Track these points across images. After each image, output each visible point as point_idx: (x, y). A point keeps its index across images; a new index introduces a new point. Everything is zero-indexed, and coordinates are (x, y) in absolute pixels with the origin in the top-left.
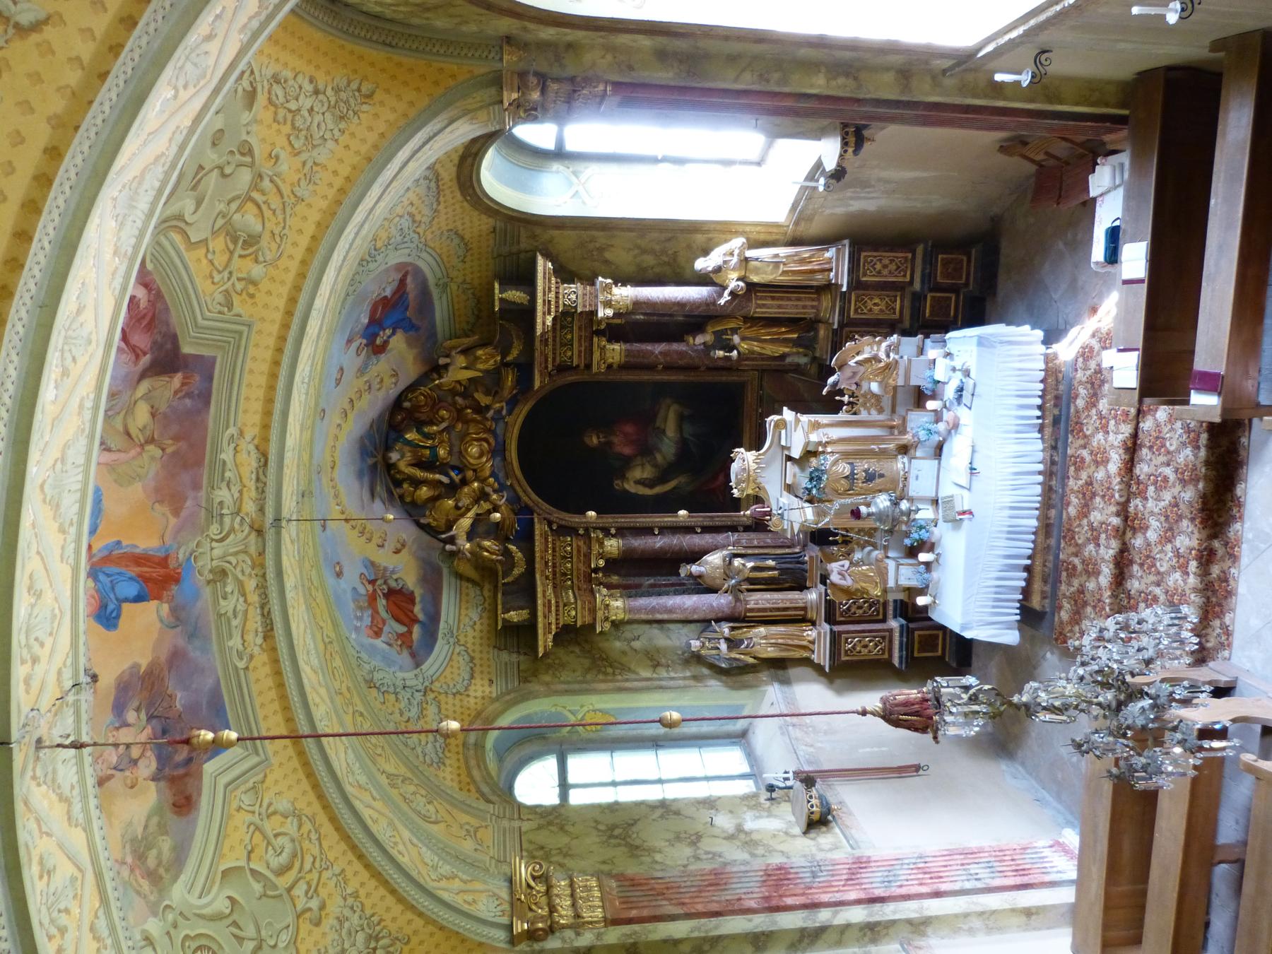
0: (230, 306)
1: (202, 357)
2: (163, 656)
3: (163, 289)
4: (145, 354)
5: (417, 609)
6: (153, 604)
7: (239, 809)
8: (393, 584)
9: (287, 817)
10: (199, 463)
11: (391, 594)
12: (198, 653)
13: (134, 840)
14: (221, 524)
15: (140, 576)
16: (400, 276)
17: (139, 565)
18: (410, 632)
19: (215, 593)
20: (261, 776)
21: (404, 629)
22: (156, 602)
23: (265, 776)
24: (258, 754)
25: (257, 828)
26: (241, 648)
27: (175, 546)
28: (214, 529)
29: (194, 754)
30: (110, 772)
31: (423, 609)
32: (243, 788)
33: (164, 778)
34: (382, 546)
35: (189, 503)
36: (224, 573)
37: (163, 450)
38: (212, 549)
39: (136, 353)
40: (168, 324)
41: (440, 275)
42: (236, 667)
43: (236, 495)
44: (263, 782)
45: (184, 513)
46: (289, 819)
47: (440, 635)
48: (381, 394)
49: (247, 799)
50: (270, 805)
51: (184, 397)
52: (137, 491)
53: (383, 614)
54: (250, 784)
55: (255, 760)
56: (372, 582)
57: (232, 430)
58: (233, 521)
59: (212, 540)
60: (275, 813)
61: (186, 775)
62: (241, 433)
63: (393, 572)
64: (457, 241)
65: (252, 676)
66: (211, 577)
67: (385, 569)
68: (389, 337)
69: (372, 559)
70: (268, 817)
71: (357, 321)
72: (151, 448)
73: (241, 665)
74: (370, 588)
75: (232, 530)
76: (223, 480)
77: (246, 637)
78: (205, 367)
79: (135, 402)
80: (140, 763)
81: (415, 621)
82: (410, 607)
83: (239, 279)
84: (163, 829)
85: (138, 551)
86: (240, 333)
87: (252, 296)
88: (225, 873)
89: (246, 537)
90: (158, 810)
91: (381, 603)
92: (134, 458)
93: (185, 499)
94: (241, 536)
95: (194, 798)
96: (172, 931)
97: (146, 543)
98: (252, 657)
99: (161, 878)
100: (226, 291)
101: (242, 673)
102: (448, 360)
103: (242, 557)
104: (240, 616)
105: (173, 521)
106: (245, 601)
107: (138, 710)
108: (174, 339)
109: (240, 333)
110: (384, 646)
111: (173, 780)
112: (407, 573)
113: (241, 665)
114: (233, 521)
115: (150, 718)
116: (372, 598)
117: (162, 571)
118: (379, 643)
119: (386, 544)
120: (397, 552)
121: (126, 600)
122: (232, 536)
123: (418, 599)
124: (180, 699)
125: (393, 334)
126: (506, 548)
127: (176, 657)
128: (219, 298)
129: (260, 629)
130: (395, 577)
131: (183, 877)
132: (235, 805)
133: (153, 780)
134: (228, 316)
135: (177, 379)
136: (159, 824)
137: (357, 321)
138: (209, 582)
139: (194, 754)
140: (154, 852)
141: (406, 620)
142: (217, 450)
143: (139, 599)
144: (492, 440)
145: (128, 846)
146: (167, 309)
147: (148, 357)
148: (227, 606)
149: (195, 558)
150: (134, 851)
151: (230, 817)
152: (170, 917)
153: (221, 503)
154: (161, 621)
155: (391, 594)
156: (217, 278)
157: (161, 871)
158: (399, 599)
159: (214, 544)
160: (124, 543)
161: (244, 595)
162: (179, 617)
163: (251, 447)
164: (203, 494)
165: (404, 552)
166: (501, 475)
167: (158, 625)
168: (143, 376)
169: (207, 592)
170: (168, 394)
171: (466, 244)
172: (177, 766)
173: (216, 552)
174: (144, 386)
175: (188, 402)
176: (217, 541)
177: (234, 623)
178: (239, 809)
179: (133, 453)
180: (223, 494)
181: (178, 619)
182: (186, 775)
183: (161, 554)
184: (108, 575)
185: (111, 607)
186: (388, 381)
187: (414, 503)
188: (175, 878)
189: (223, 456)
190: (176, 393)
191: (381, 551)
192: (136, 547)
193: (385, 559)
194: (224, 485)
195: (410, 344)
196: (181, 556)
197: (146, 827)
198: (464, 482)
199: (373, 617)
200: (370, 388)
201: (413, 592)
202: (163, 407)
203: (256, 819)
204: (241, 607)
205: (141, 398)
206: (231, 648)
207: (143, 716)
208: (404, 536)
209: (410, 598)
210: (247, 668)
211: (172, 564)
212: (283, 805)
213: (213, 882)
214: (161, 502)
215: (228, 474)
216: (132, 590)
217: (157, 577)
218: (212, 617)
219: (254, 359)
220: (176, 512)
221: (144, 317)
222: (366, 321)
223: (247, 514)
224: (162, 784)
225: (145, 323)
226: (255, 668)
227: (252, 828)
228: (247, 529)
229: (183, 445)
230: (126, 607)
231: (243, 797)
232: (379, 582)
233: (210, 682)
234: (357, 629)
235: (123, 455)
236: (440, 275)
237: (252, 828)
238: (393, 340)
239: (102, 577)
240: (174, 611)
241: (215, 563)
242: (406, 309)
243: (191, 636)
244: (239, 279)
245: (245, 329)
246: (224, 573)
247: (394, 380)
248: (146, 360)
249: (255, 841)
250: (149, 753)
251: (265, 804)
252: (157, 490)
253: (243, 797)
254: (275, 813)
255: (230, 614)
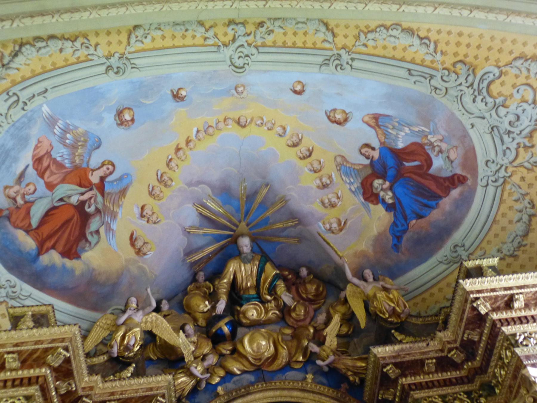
5: (53, 258)
8: (94, 224)
11: (82, 214)
16: (459, 171)
18: (28, 230)
21: (35, 222)
31: (52, 267)
34: (142, 216)
41: (467, 245)
47: (14, 279)
48: (317, 208)
53: (63, 190)
56: (101, 187)
63: (109, 229)
64: (520, 228)
67: (114, 216)
68: (383, 202)
69: (129, 193)
71: (402, 124)
74: (95, 179)
81: (41, 250)
82: (61, 246)
91: (73, 193)
102: (371, 279)
110: (20, 168)
112: (104, 254)
116: (79, 176)
118: (26, 159)
119: (144, 222)
120: (133, 240)
123: (69, 263)
125: (389, 208)
126: (129, 364)
130: (102, 230)
137: (402, 124)
141: (47, 230)
144: (275, 367)
155: (82, 214)
158: (70, 228)
165: (130, 252)
166: (230, 385)
171: (520, 245)
186: (332, 216)
187: (185, 292)
191: (137, 211)
193: (126, 218)
195: (378, 239)
198: (217, 339)
199: (60, 166)
200: (324, 186)
201: (78, 257)
208: (150, 254)
209: (71, 253)
222: (400, 145)
232: (99, 198)
234: (51, 122)
236: (467, 245)
238: (379, 209)
242: (420, 217)
247: (335, 225)
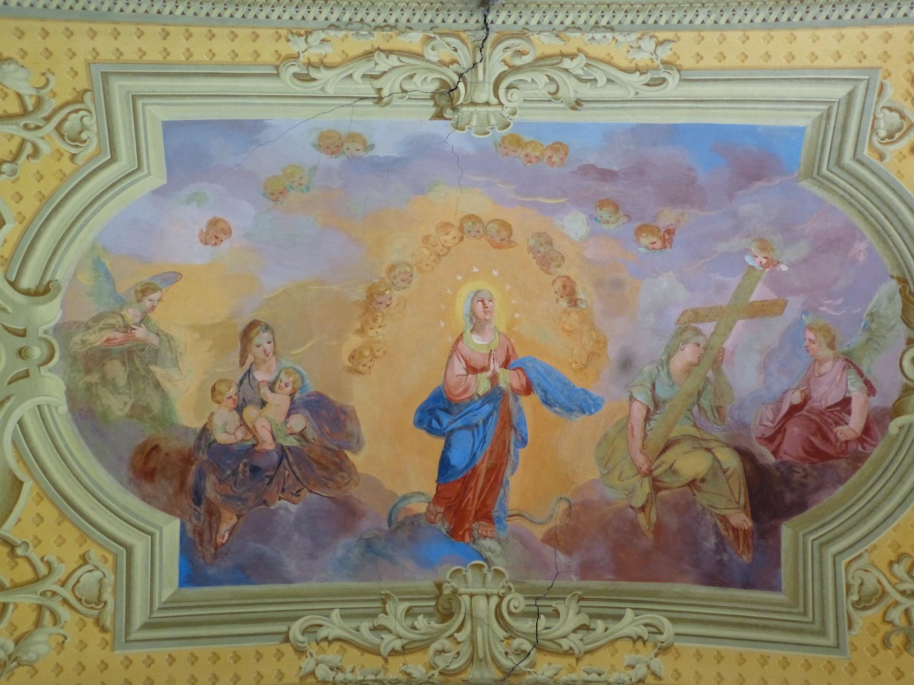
0: (863, 604)
1: (778, 564)
2: (355, 492)
3: (866, 467)
4: (775, 453)
6: (431, 489)
7: (84, 559)
9: (17, 642)
10: (622, 572)
12: (340, 552)
13: (155, 356)
14: (525, 615)
15: (474, 470)
17: (489, 471)
19: (420, 595)
20: (108, 624)
22: (431, 490)
23: (103, 629)
24: (146, 626)
25: (38, 579)
26: (322, 633)
27: (503, 535)
28: (518, 602)
29: (202, 510)
30: (250, 359)
32: (110, 579)
33: (197, 448)
35: (562, 558)
36: (447, 615)
37: (643, 508)
38: (488, 596)
39: (773, 439)
40: (819, 487)
42: (296, 618)
43: (565, 644)
44: (97, 621)
45: (548, 550)
46: (11, 646)
49: (89, 579)
50: (56, 619)
51: (718, 534)
52: (588, 471)
54: (108, 596)
55: (138, 619)
57: (669, 629)
58: (525, 635)
59: (501, 598)
60: (38, 623)
61: (182, 484)
62: (663, 650)
65: (269, 647)
66: (447, 592)
70: (40, 607)
72: (646, 488)
73: (295, 629)
75: (512, 633)
76: (592, 616)
77: (337, 645)
78: (762, 575)
79: (708, 450)
80: (236, 416)
83: (907, 612)
84: (139, 412)
85: (508, 471)
86: (823, 633)
87: (886, 643)
88: (18, 484)
89: (494, 659)
90: (164, 420)
92: (633, 461)
93: (569, 553)
94: (499, 650)
95: (148, 487)
96: (20, 342)
97: (517, 488)
98: (300, 652)
99: (88, 371)
100: (884, 593)
101: (281, 628)
103: (466, 650)
104: (373, 638)
105: (539, 532)
106: (394, 652)
107: (302, 435)
108: (800, 506)
109: (823, 633)
111: (187, 459)
113: (295, 629)
114: (525, 635)
115: (283, 451)
117: (472, 508)
121: (448, 446)
122: (502, 633)
124: (287, 508)
127: (348, 513)
128: (871, 583)
129: (340, 677)
131: (64, 408)
132: (95, 554)
133: (204, 429)
134: (846, 604)
135: (741, 520)
136: (148, 409)
138: (439, 586)
139: (202, 510)
140: (122, 381)
142: (639, 601)
143: (445, 464)
145: (154, 340)
146: (841, 481)
147: (771, 459)
148: (395, 617)
149: (480, 567)
150: (143, 346)
151: (84, 537)
152: (37, 352)
153: (556, 614)
154: (405, 498)
156: (900, 570)
157: (94, 378)
159: (494, 600)
160: (522, 452)
161: (404, 651)
162: (403, 528)
163: (641, 671)
164: (574, 582)
167: (400, 493)
168: (746, 455)
169: (426, 583)
170: (722, 505)
172: (201, 475)
173: (481, 602)
174: (730, 460)
175: (711, 542)
176: (499, 606)
177: (365, 626)
178: (84, 559)
179: (641, 459)
180: (571, 617)
181: (401, 525)
182: (182, 484)
183: (495, 514)
184: (485, 422)
185: (445, 419)
188: (70, 394)
189: (629, 614)
190: (724, 519)
192: (514, 470)
194: (584, 619)
196: (487, 543)
197: (157, 385)
202: (703, 499)
203: (50, 585)
204: (389, 642)
205: (716, 459)
206: (327, 614)
207: (291, 442)
210: (287, 640)
211: (479, 527)
212: (41, 645)
213: (20, 458)
214: (569, 513)
215: (600, 625)
216: (458, 459)
217: (466, 500)
218: (385, 585)
219: (785, 663)
220: (551, 538)
221: (825, 438)
223: (533, 665)
224: (191, 441)
225: (816, 441)
226: (280, 655)
227: (43, 570)
228: (507, 663)
229: (648, 541)
230: (439, 443)
231: (98, 574)
233: (291, 565)
235: (638, 443)
237: (43, 570)
239: (487, 408)
240: (413, 523)
241: (465, 599)
243: (368, 545)
244: (907, 612)
245: (831, 641)
246: (447, 615)
248: (767, 457)
249: (23, 565)
250: (240, 435)
251: (65, 613)
252: (586, 506)
253: (98, 574)
254: (38, 623)
255: (382, 620)
